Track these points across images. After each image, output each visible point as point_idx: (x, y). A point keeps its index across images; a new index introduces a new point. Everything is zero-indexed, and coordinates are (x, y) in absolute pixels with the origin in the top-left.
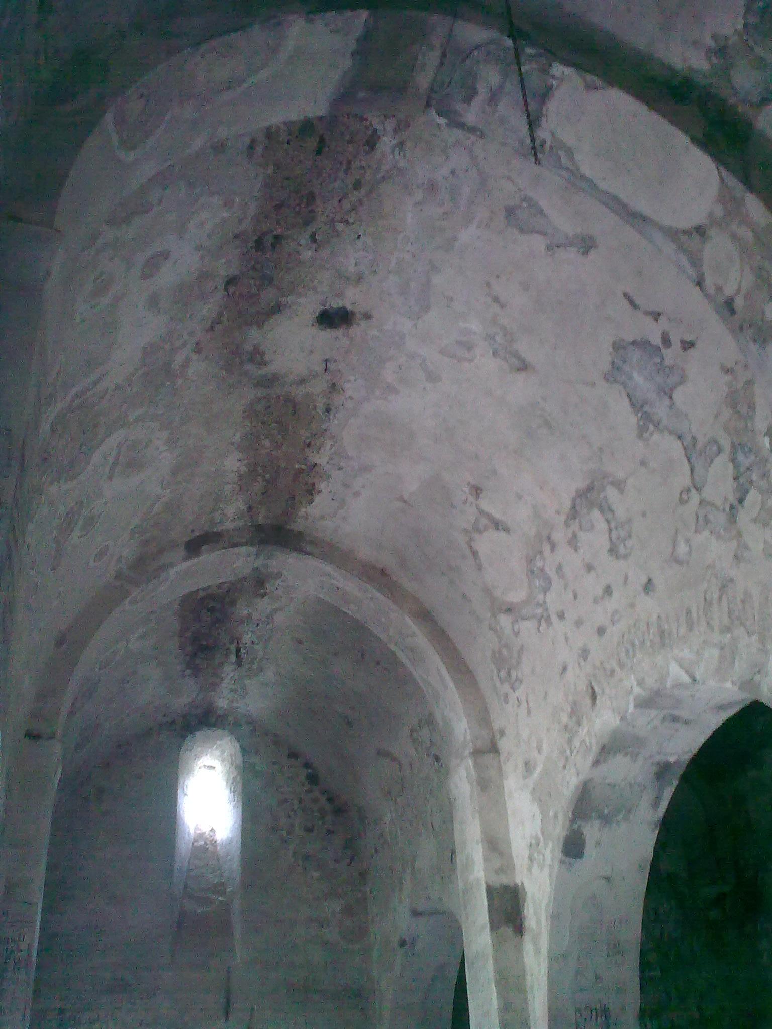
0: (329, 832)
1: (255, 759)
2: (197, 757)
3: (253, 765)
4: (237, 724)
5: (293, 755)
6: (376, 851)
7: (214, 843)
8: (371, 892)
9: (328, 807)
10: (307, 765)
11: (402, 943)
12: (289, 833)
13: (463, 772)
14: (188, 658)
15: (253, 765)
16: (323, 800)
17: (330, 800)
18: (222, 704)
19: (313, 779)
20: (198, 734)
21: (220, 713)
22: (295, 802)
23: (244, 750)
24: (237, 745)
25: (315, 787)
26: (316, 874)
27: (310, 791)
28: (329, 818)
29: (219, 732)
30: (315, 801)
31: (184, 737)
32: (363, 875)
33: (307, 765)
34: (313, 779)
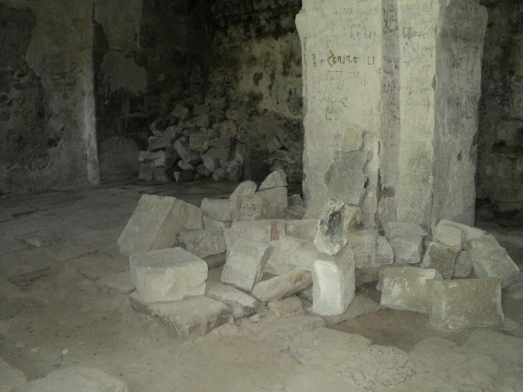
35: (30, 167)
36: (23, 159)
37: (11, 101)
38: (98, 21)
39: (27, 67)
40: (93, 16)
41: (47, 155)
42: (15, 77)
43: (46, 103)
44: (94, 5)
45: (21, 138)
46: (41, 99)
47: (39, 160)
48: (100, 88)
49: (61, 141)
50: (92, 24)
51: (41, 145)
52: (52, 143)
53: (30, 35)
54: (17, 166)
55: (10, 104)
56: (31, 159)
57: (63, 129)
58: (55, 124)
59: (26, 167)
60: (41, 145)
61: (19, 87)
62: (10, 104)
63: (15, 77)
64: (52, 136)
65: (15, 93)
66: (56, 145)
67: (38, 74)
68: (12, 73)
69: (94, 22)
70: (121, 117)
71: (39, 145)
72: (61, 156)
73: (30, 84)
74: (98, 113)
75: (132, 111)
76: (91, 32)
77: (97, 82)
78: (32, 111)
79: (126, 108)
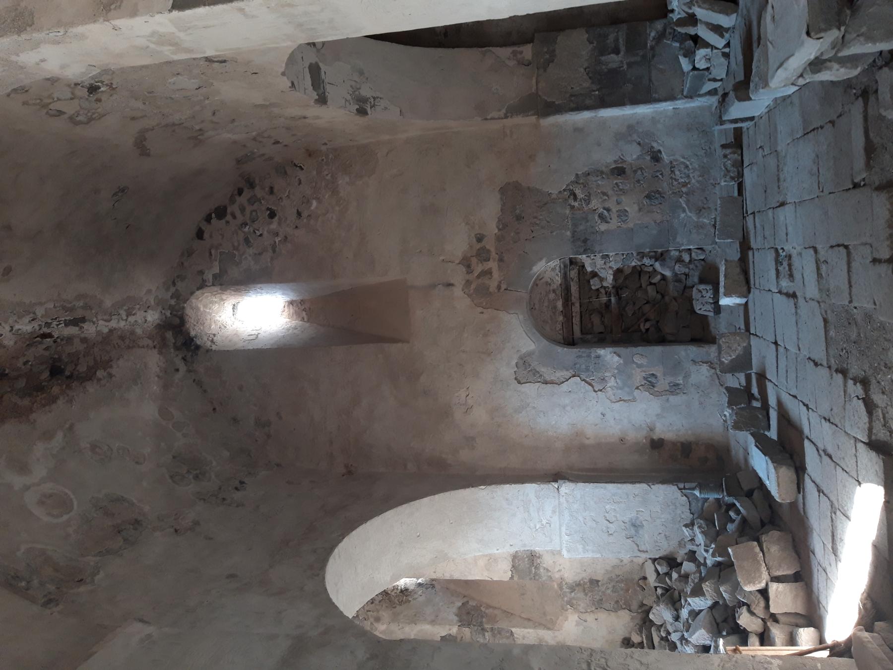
0: (272, 191)
1: (209, 276)
2: (223, 327)
3: (215, 276)
4: (176, 296)
5: (200, 235)
6: (277, 142)
7: (302, 302)
8: (325, 144)
9: (247, 194)
10: (208, 219)
11: (362, 112)
12: (277, 234)
13: (28, 58)
14: (75, 384)
15: (215, 276)
16: (243, 200)
17: (240, 192)
18: (153, 317)
19: (221, 212)
20: (193, 333)
21: (168, 314)
22: (246, 229)
23: (202, 286)
24: (198, 293)
25: (229, 210)
26: (314, 203)
27: (234, 217)
28: (259, 192)
29: (189, 311)
30: (243, 210)
31: (198, 347)
32: (310, 154)
33: (208, 219)
34: (221, 212)
35: (685, 185)
36: (673, 193)
37: (604, 209)
38: (504, 111)
39: (564, 190)
40: (499, 118)
41: (671, 162)
42: (576, 204)
43: (607, 167)
44: (486, 119)
45: (648, 197)
46: (602, 172)
47: (677, 173)
48: (588, 102)
49: (655, 145)
50: (509, 120)
51: (658, 171)
52: (656, 157)
53: (529, 188)
54: (682, 201)
55: (608, 210)
56: (675, 183)
57: (639, 144)
58: (632, 154)
59: (684, 190)
60: (658, 171)
61: (588, 201)
62: (608, 210)
63: (576, 204)
64: (648, 158)
65: (595, 203)
66: (660, 151)
67: (573, 178)
68: (572, 207)
69: (506, 117)
70: (625, 67)
71: (658, 174)
72: (673, 147)
73: (585, 186)
74: (620, 103)
75: (617, 51)
76: (519, 120)
77: (580, 108)
78: (616, 184)
79: (613, 60)
